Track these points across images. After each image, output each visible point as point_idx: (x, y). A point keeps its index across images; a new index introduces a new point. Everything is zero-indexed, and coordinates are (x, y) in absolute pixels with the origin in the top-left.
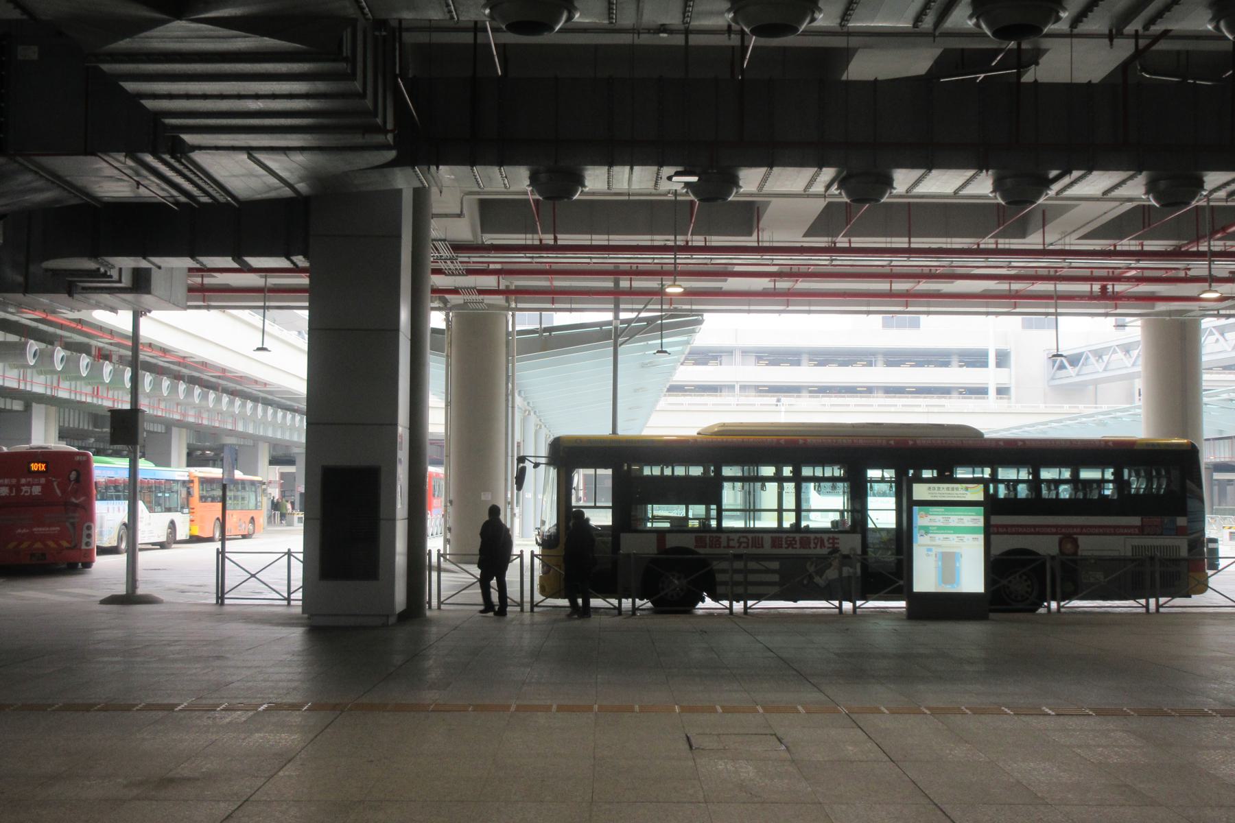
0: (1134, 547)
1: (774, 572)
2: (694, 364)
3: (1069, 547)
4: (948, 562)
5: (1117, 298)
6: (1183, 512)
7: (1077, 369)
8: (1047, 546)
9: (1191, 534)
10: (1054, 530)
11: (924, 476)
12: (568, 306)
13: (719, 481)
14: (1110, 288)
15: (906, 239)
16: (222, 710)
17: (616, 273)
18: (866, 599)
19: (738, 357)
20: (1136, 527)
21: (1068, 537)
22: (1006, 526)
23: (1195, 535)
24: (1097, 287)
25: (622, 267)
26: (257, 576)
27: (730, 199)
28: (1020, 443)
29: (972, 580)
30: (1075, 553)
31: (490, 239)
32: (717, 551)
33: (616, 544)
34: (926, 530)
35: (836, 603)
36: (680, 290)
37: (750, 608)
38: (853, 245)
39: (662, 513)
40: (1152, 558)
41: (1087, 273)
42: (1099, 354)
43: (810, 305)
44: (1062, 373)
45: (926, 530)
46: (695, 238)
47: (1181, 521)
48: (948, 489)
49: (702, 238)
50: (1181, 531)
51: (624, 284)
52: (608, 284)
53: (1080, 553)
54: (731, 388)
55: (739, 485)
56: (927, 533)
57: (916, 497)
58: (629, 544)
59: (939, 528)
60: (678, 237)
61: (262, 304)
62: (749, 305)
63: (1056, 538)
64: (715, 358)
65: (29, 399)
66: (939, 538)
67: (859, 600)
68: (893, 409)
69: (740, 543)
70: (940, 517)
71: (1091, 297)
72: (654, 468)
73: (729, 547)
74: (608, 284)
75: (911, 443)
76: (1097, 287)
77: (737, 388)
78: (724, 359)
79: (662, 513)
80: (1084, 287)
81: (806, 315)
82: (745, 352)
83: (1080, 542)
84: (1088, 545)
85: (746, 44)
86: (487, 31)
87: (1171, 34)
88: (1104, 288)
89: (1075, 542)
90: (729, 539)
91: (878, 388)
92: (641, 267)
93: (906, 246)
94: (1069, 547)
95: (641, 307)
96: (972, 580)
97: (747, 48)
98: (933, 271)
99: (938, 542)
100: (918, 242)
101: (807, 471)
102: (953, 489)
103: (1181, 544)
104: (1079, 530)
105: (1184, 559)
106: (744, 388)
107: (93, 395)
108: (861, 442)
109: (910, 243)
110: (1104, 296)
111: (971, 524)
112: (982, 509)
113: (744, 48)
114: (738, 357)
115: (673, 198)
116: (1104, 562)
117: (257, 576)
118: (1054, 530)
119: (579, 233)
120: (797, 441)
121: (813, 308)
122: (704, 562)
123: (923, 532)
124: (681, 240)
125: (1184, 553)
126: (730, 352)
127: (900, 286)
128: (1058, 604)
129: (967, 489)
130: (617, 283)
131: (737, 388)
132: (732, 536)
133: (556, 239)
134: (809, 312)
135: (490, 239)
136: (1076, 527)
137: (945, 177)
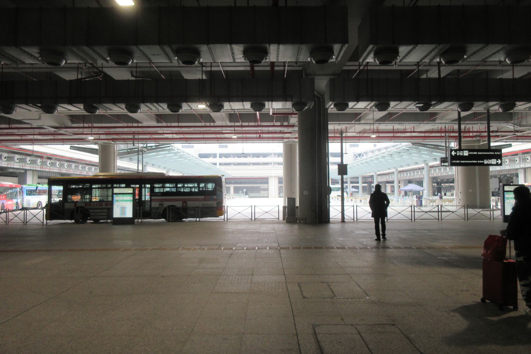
0: (202, 204)
1: (105, 212)
2: (263, 157)
3: (185, 204)
4: (123, 209)
5: (263, 138)
6: (215, 194)
7: (360, 157)
8: (179, 204)
9: (218, 200)
10: (181, 200)
11: (93, 187)
12: (205, 142)
13: (91, 189)
14: (261, 136)
15: (254, 123)
16: (122, 250)
17: (134, 133)
18: (144, 219)
19: (273, 155)
20: (202, 199)
21: (185, 202)
22: (168, 199)
23: (219, 201)
24: (258, 136)
25: (136, 132)
26: (36, 216)
27: (97, 113)
28: (173, 177)
29: (129, 214)
30: (186, 206)
31: (74, 125)
32: (91, 207)
33: (63, 206)
34: (117, 201)
35: (195, 219)
36: (93, 138)
37: (48, 223)
38: (249, 125)
39: (77, 198)
40: (198, 207)
41: (255, 132)
42: (366, 153)
43: (268, 141)
44: (357, 158)
45: (117, 201)
46: (276, 123)
47: (215, 197)
48: (123, 190)
49: (209, 124)
50: (215, 200)
51: (137, 137)
52: (131, 137)
53: (188, 206)
54: (271, 163)
55: (97, 190)
56: (118, 202)
57: (114, 192)
58: (67, 206)
59: (121, 200)
60: (256, 123)
61: (138, 143)
62: (253, 141)
63: (181, 202)
64: (267, 156)
65: (26, 170)
66: (121, 203)
67: (48, 220)
68: (265, 169)
69: (97, 205)
70: (120, 197)
71: (256, 138)
72: (117, 185)
73: (93, 206)
74: (131, 137)
75: (144, 177)
76: (258, 136)
77: (273, 164)
78: (270, 156)
79: (77, 198)
80: (255, 136)
81: (268, 144)
82: (275, 154)
83: (188, 203)
84: (190, 204)
85: (285, 69)
86: (220, 67)
87: (369, 64)
88: (260, 136)
89: (186, 203)
90: (94, 204)
91: (232, 164)
92: (111, 132)
93: (254, 125)
94: (185, 204)
95: (145, 143)
96: (129, 214)
97: (285, 70)
98: (257, 132)
99: (120, 204)
100: (180, 124)
101: (115, 185)
102: (125, 190)
103: (214, 204)
104: (188, 200)
105: (215, 207)
106: (274, 163)
107: (41, 168)
108: (130, 177)
109: (214, 124)
110: (260, 138)
111: (129, 199)
112: (132, 195)
113: (284, 70)
114: (273, 155)
115: (234, 113)
116: (194, 208)
117: (36, 216)
118: (181, 200)
119: (189, 123)
120: (113, 178)
121: (269, 142)
122: (87, 210)
123: (116, 201)
124: (272, 124)
125: (215, 205)
126: (271, 154)
127: (244, 136)
128: (199, 219)
129: (128, 190)
130: (134, 136)
131: (273, 164)
132: (95, 203)
133: (138, 125)
134: (268, 143)
135: (74, 125)
136: (187, 199)
137: (71, 107)
